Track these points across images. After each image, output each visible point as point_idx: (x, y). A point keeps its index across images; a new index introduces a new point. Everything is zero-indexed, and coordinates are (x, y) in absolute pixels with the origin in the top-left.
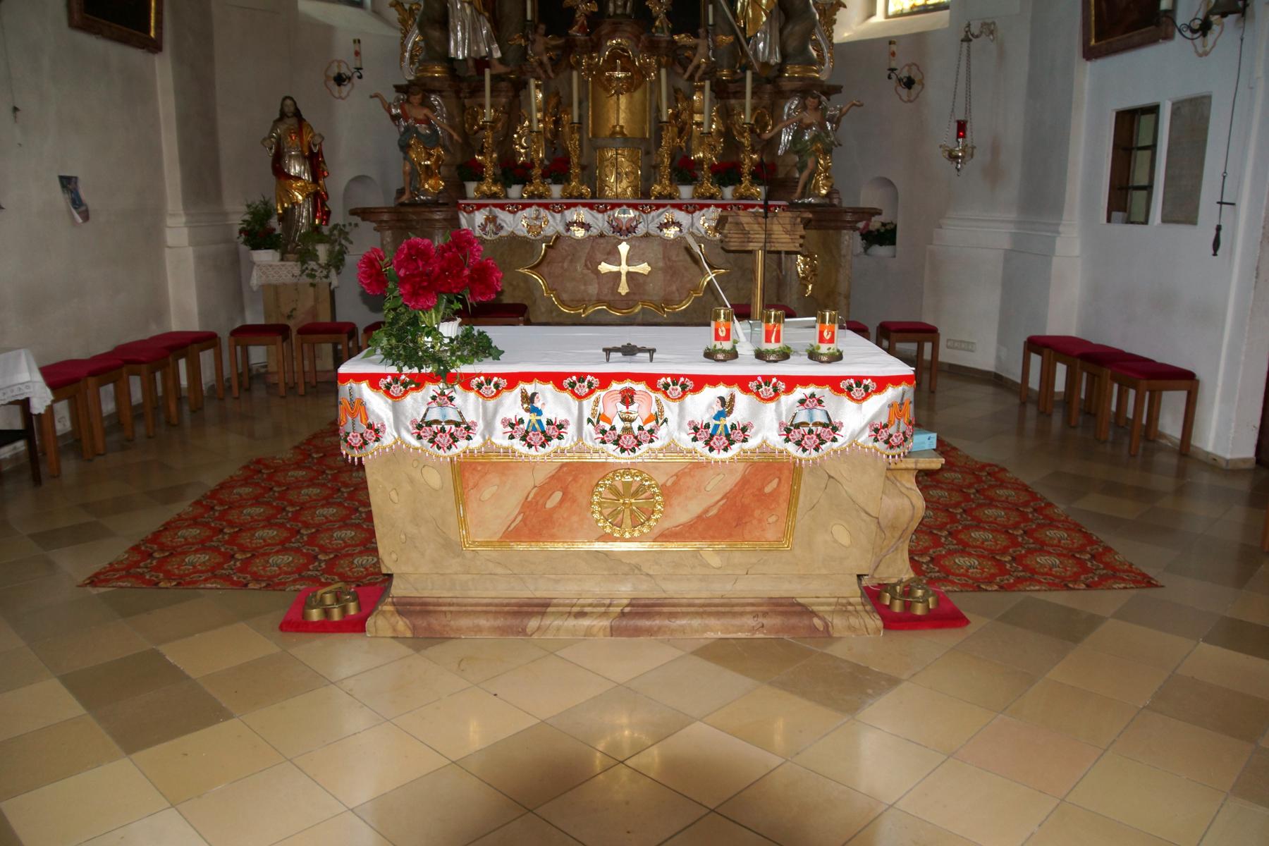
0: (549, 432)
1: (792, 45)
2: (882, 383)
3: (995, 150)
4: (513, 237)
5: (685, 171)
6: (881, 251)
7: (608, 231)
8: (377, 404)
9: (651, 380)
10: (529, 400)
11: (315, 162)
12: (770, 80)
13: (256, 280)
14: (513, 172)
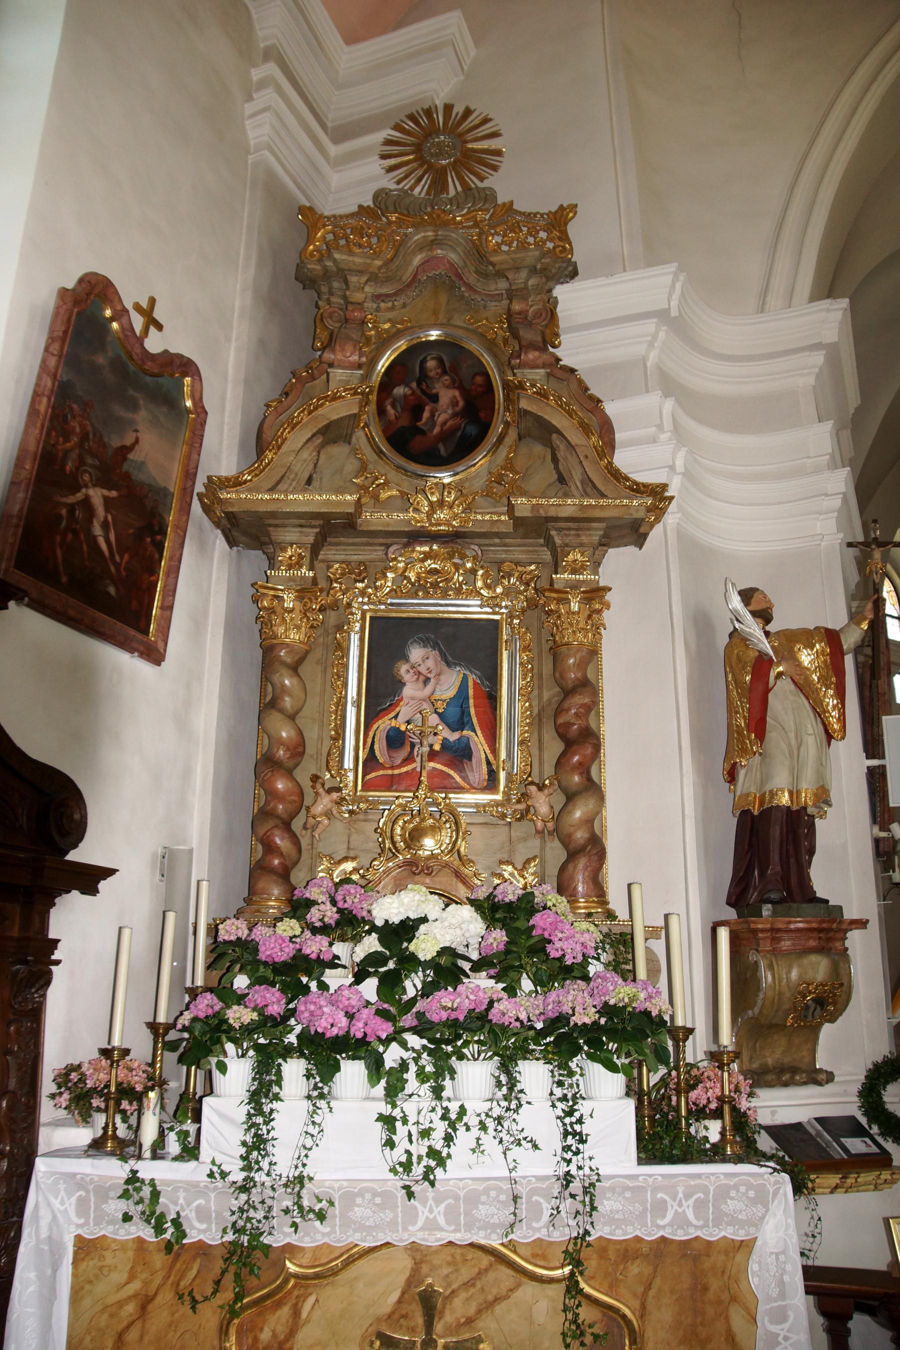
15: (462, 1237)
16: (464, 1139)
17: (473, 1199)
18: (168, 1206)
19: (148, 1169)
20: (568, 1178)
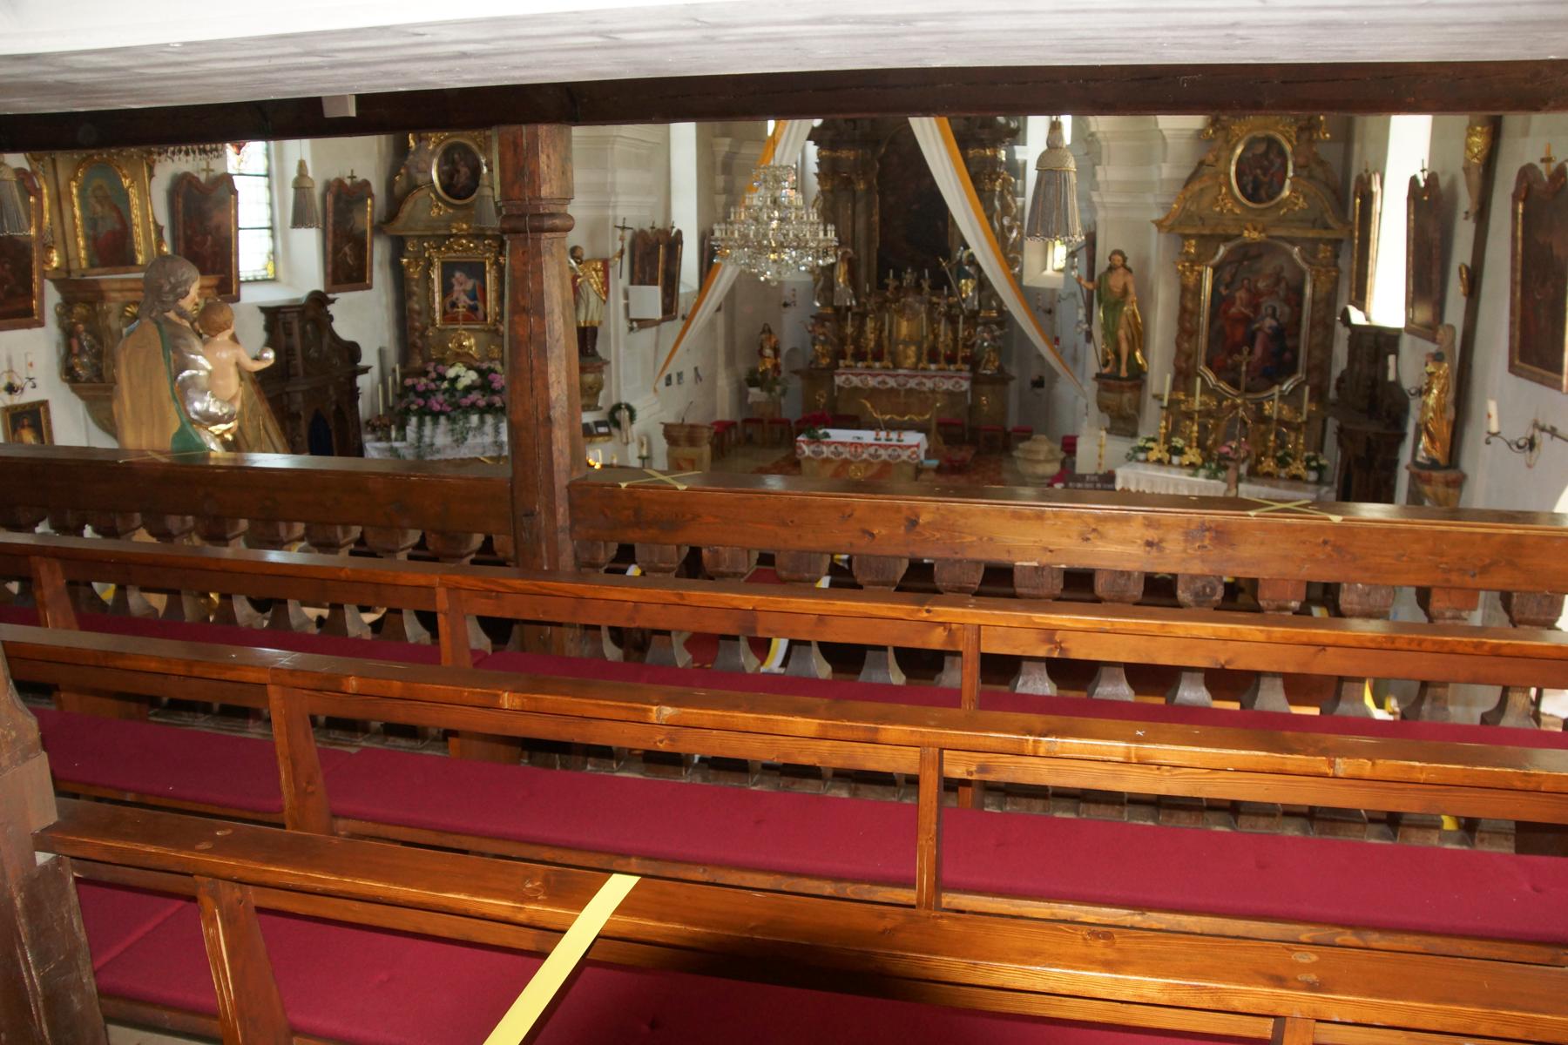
0: (840, 454)
1: (984, 302)
2: (909, 447)
3: (1076, 350)
4: (856, 389)
5: (933, 356)
6: (1039, 391)
7: (895, 385)
8: (805, 447)
9: (861, 444)
10: (836, 448)
11: (776, 351)
12: (972, 318)
13: (750, 400)
14: (860, 356)
15: (473, 456)
16: (471, 434)
17: (474, 447)
18: (403, 452)
19: (397, 444)
20: (496, 442)
